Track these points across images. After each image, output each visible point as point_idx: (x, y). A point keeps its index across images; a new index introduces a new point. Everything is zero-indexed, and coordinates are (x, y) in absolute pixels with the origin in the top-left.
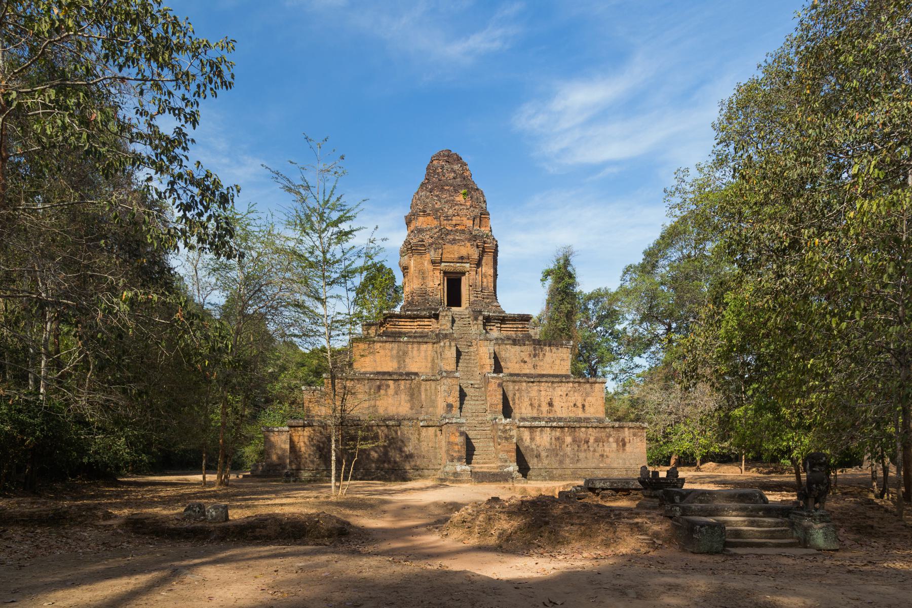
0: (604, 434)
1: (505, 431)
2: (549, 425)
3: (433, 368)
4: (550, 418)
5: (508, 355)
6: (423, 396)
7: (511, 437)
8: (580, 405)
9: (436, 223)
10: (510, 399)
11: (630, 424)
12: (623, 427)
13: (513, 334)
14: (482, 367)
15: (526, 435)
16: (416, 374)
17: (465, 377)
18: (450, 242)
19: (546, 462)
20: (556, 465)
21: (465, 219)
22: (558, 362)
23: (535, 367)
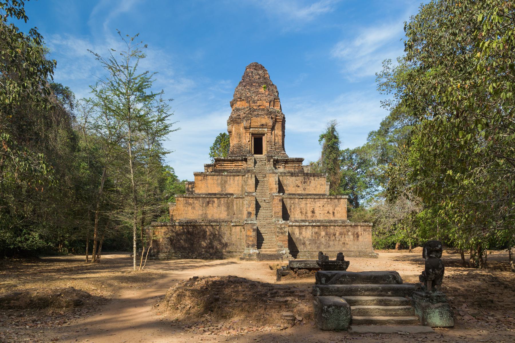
0: (345, 230)
1: (281, 229)
3: (242, 191)
4: (312, 221)
5: (288, 182)
6: (235, 208)
7: (285, 232)
8: (331, 212)
10: (288, 209)
11: (362, 224)
12: (357, 226)
13: (292, 170)
14: (271, 189)
15: (297, 231)
16: (232, 194)
17: (260, 196)
18: (255, 116)
19: (309, 247)
21: (264, 102)
22: (319, 186)
23: (304, 189)
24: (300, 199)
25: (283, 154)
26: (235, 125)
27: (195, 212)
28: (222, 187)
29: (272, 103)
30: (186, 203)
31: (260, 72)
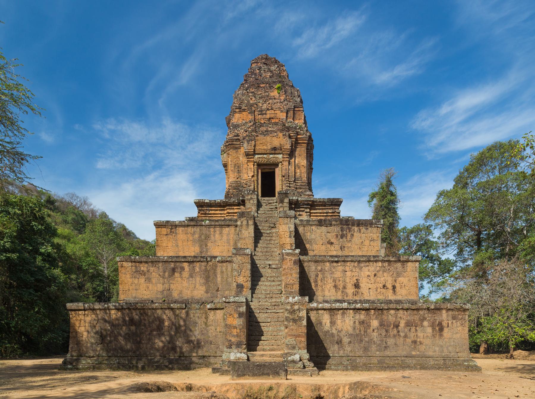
0: (416, 318)
1: (293, 312)
2: (353, 306)
5: (313, 236)
6: (219, 279)
8: (389, 286)
9: (251, 117)
14: (282, 246)
15: (326, 318)
17: (263, 258)
19: (349, 349)
20: (361, 353)
22: (367, 243)
24: (333, 262)
26: (232, 152)
27: (150, 288)
28: (201, 246)
29: (291, 113)
30: (136, 271)
31: (273, 68)
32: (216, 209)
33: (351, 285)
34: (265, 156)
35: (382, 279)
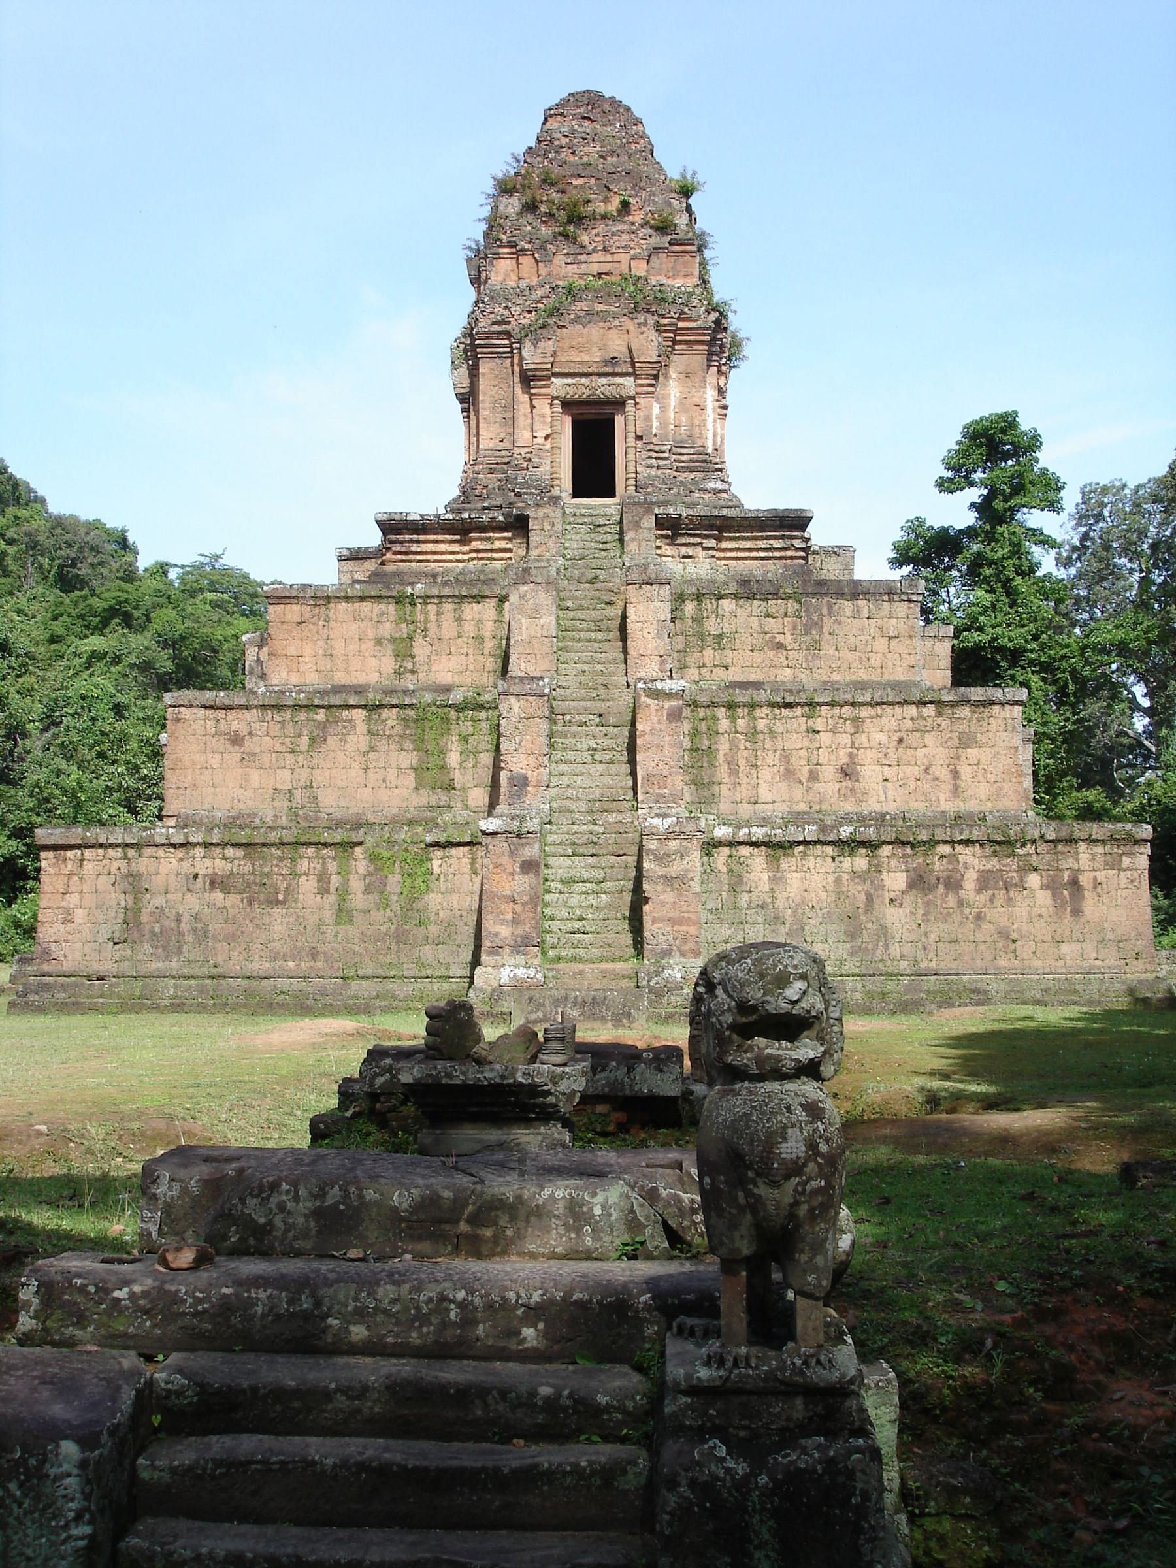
13: (752, 568)
25: (717, 492)
32: (440, 537)
33: (832, 769)
34: (583, 380)
35: (921, 752)
